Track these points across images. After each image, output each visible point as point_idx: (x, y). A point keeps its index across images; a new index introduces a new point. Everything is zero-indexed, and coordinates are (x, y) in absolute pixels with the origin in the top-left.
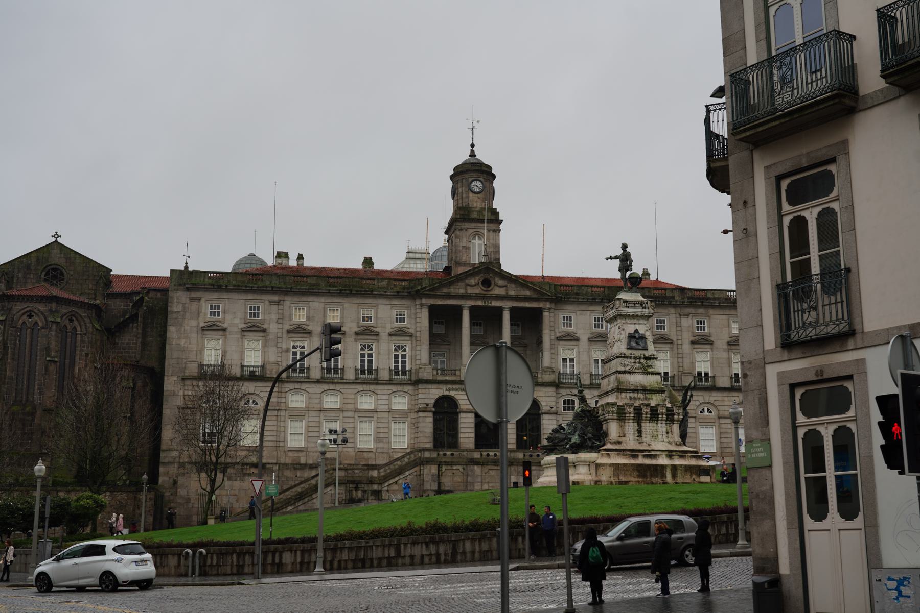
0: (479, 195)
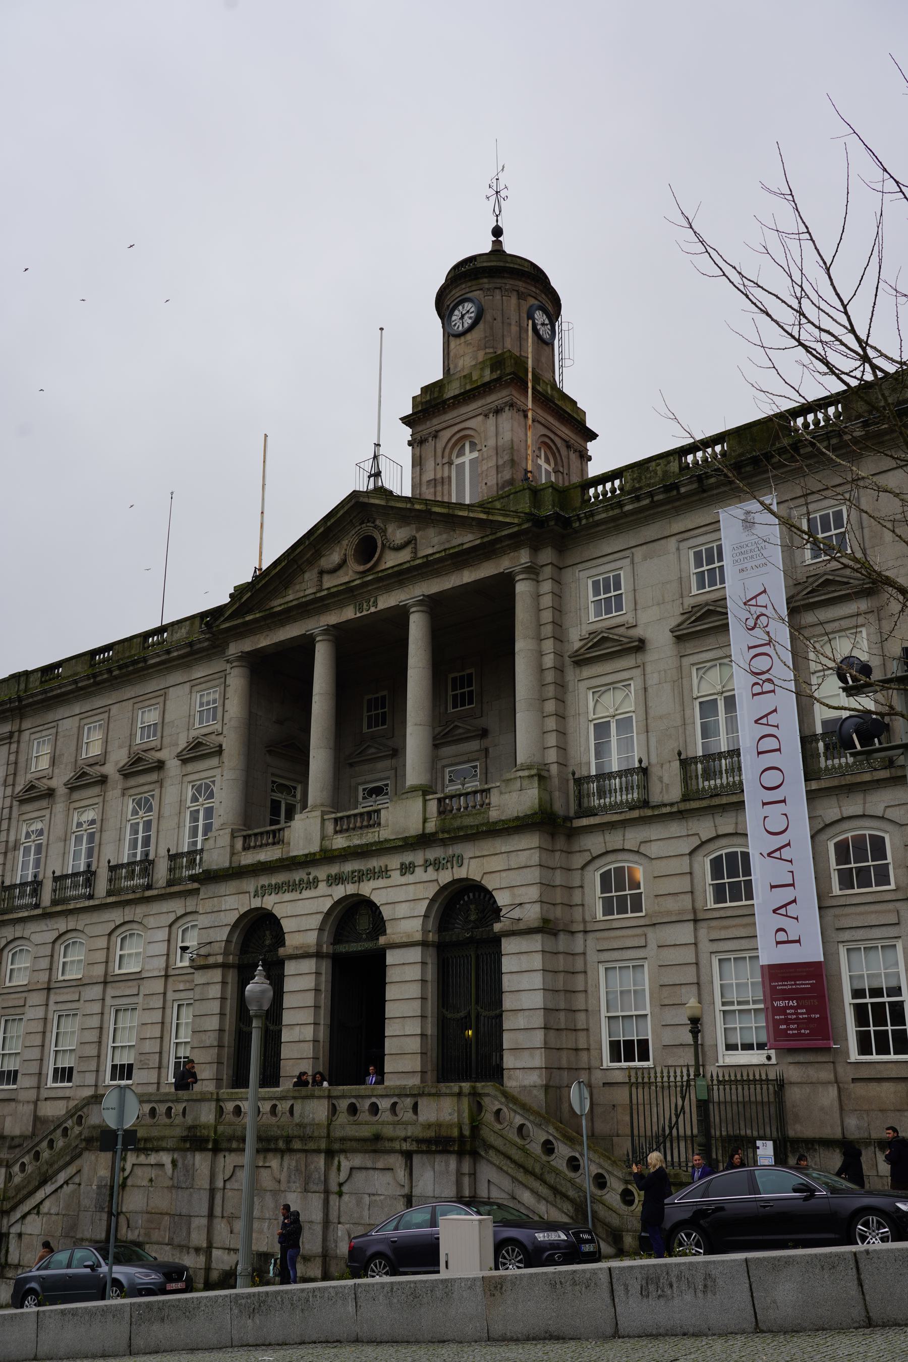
0: (469, 337)
